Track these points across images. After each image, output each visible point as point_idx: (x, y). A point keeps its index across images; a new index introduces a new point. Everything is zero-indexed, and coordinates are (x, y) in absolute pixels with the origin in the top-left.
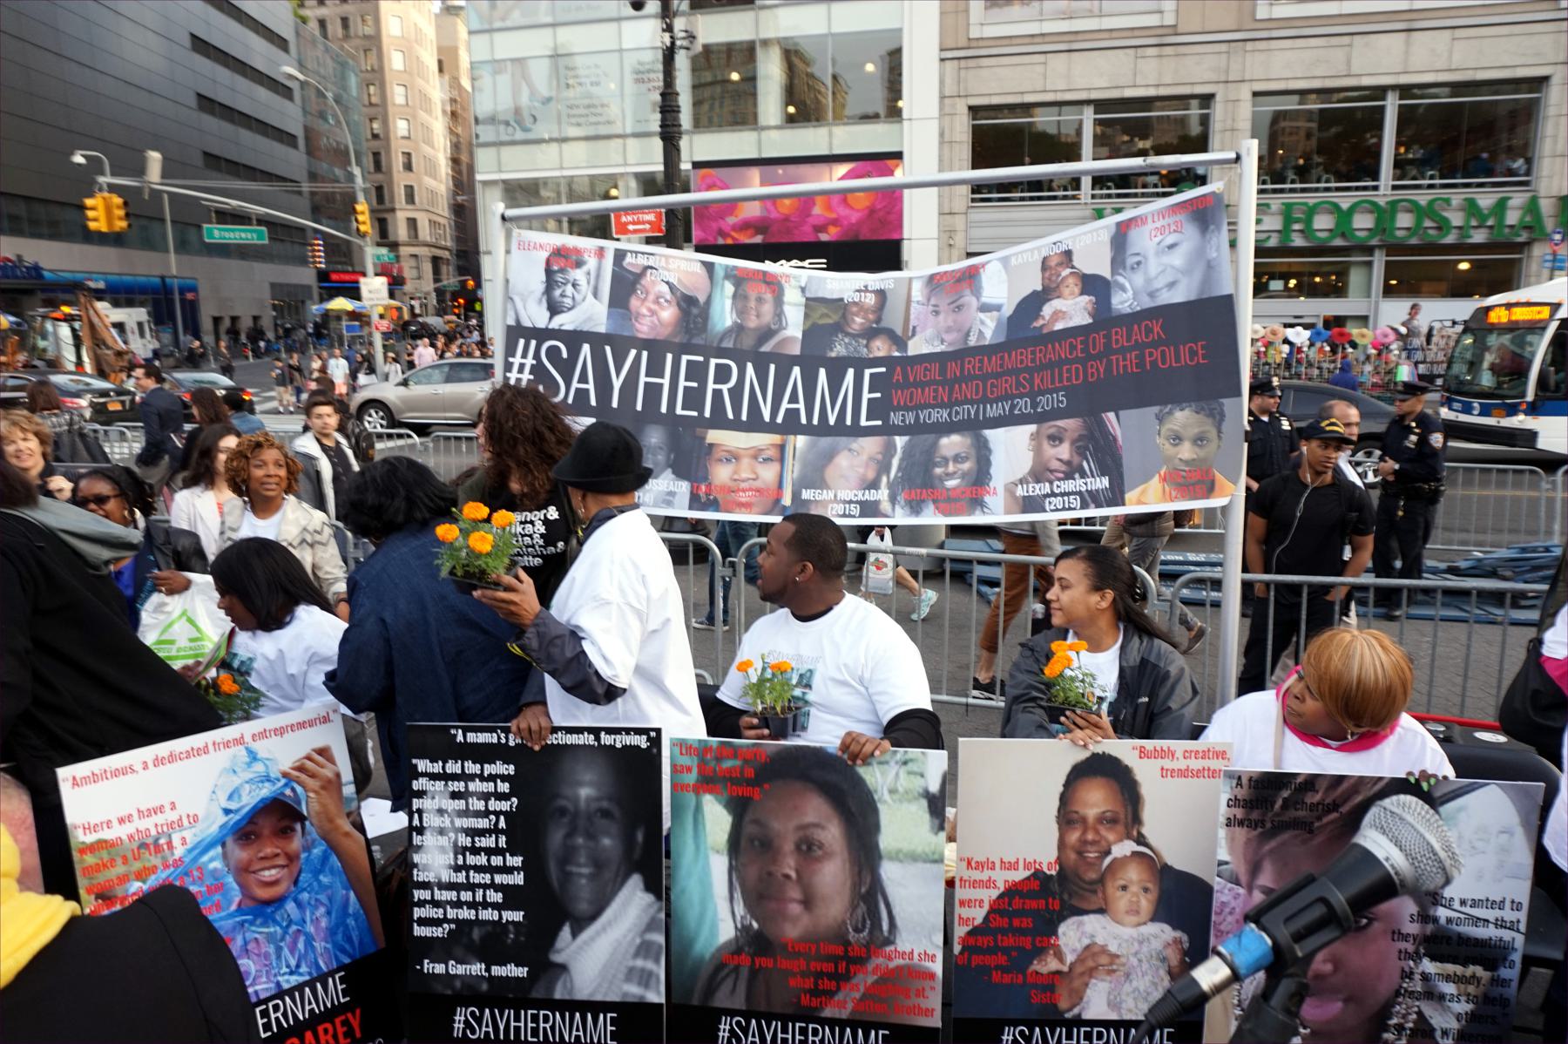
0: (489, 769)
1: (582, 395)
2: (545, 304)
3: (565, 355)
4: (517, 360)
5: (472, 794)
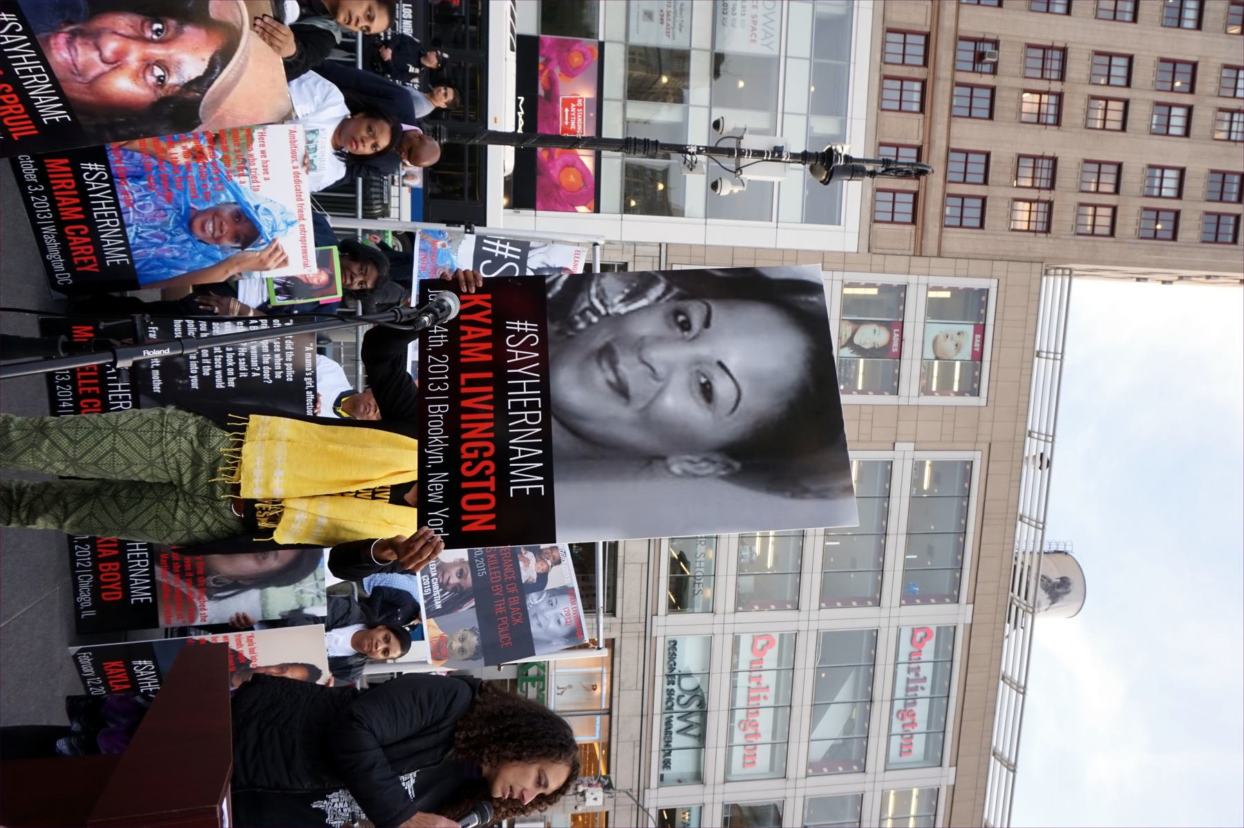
0: (289, 367)
4: (508, 247)
5: (272, 356)
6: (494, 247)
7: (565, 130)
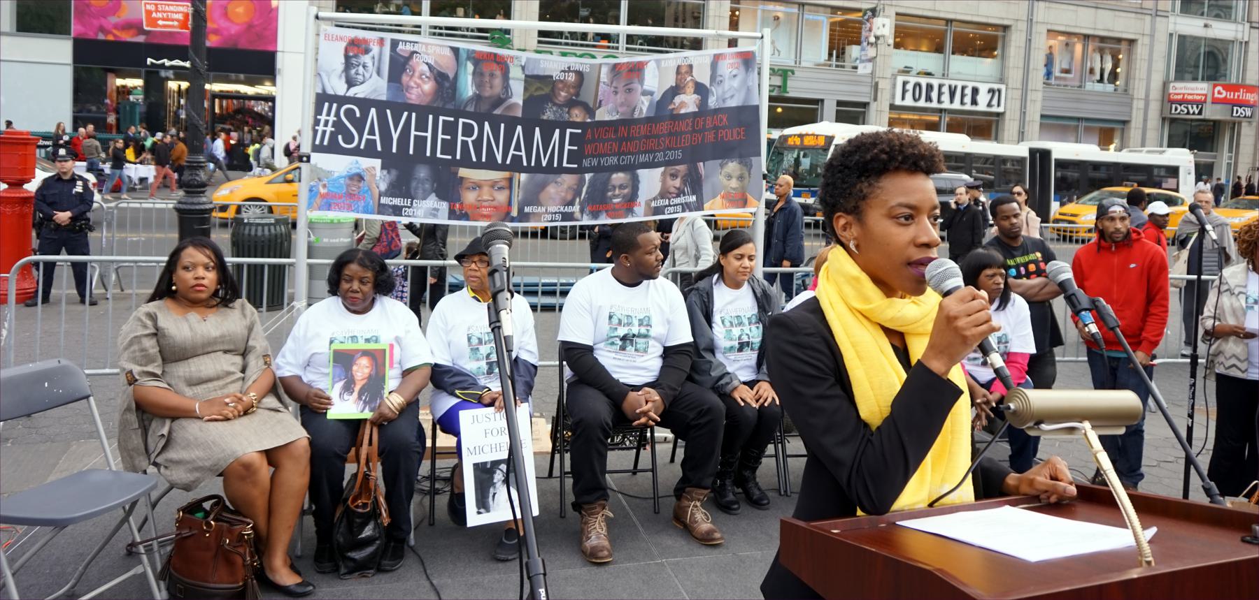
1: (371, 143)
2: (344, 79)
3: (358, 115)
4: (323, 118)
6: (324, 132)
7: (183, 24)
